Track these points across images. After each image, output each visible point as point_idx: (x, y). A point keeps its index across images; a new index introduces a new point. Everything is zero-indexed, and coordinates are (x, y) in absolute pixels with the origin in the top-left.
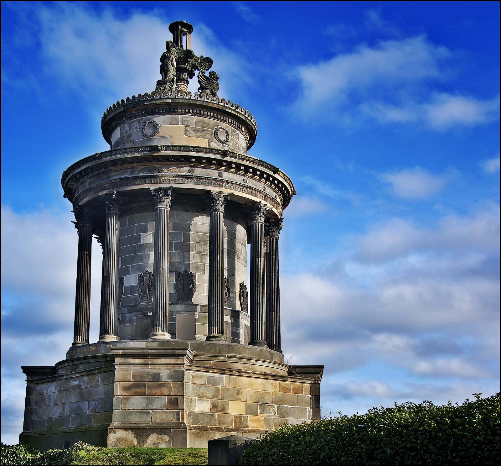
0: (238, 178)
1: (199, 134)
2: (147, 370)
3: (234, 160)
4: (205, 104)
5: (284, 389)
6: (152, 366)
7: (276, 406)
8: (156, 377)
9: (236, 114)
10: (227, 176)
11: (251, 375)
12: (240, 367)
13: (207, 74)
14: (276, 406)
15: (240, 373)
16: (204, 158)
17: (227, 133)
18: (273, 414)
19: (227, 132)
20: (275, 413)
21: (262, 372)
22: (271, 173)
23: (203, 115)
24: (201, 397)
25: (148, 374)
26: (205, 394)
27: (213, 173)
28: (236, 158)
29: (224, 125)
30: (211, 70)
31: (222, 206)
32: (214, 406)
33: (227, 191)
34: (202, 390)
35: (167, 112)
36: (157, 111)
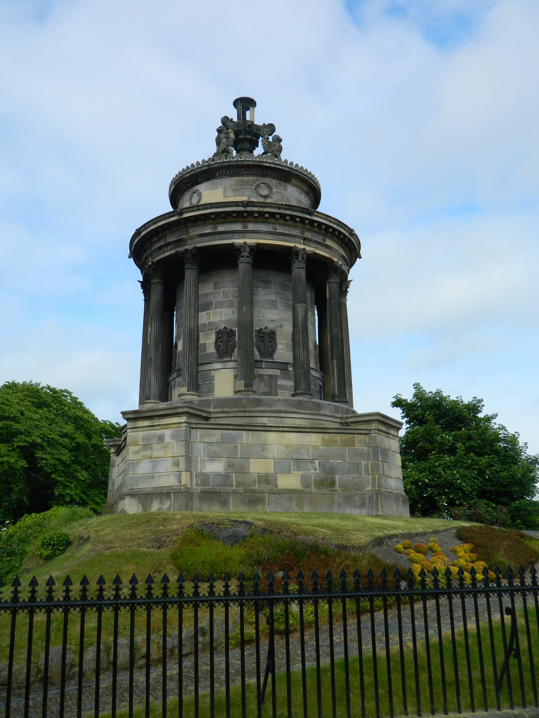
0: (264, 227)
1: (238, 193)
2: (153, 432)
3: (256, 209)
4: (239, 163)
5: (327, 443)
6: (158, 427)
7: (317, 462)
8: (161, 439)
9: (277, 166)
10: (251, 227)
11: (280, 429)
12: (265, 421)
13: (271, 139)
14: (317, 462)
15: (266, 429)
16: (222, 212)
17: (270, 188)
18: (313, 471)
19: (269, 186)
20: (315, 469)
21: (295, 424)
22: (308, 217)
23: (243, 175)
24: (213, 457)
25: (154, 436)
26: (217, 453)
27: (238, 227)
28: (256, 206)
29: (267, 180)
30: (274, 134)
31: (248, 257)
32: (230, 465)
33: (251, 241)
34: (214, 448)
35: (207, 179)
36: (199, 180)
